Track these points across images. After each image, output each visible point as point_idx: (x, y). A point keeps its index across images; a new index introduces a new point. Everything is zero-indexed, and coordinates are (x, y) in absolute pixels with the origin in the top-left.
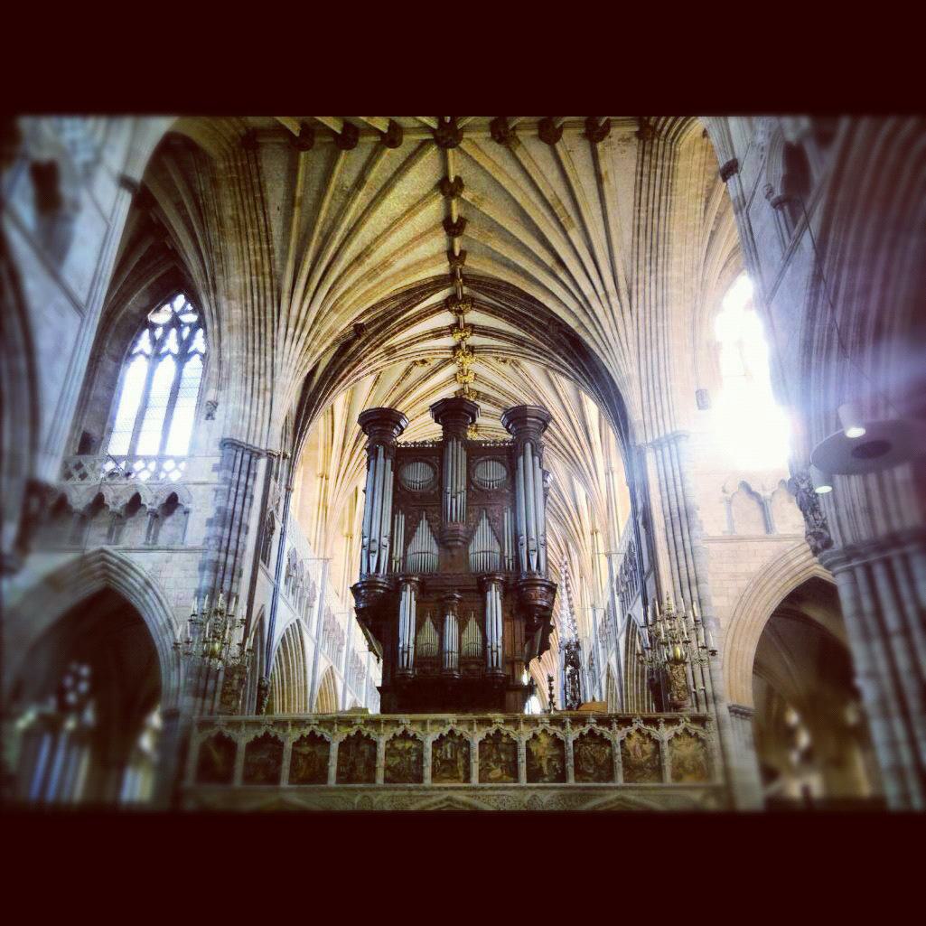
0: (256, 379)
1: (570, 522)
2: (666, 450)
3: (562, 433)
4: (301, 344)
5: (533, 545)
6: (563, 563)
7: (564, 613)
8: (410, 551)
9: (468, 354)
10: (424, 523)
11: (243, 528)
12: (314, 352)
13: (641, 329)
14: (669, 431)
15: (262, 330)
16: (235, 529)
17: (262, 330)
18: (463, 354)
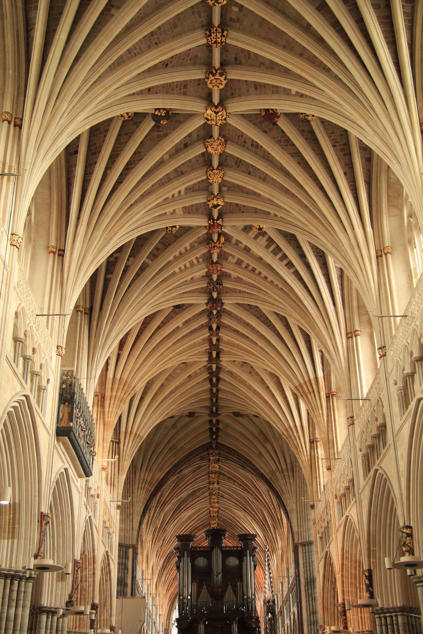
0: (126, 511)
1: (270, 533)
2: (307, 547)
3: (264, 500)
4: (144, 491)
5: (250, 600)
6: (266, 551)
7: (267, 586)
8: (199, 601)
9: (216, 462)
10: (205, 587)
11: (126, 585)
12: (150, 491)
13: (298, 487)
14: (308, 540)
15: (129, 487)
16: (122, 586)
17: (129, 487)
18: (214, 463)
